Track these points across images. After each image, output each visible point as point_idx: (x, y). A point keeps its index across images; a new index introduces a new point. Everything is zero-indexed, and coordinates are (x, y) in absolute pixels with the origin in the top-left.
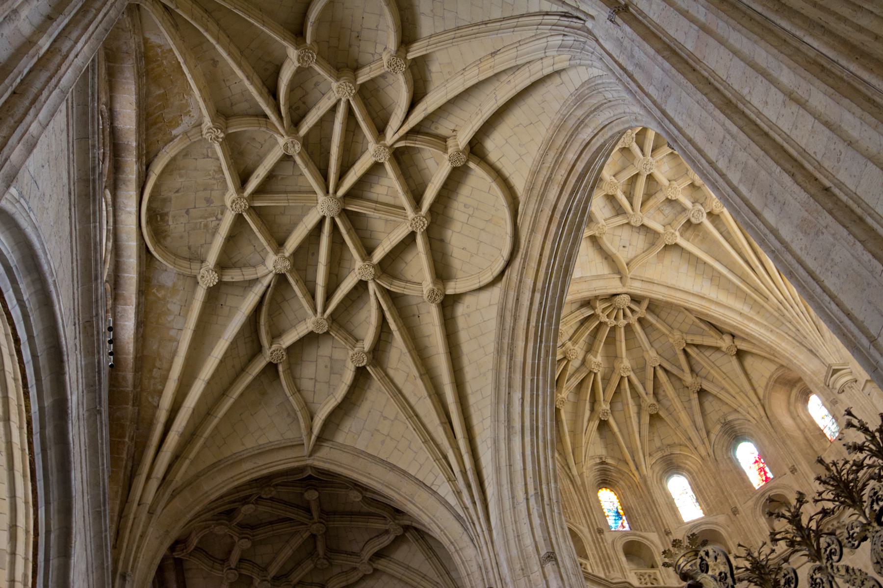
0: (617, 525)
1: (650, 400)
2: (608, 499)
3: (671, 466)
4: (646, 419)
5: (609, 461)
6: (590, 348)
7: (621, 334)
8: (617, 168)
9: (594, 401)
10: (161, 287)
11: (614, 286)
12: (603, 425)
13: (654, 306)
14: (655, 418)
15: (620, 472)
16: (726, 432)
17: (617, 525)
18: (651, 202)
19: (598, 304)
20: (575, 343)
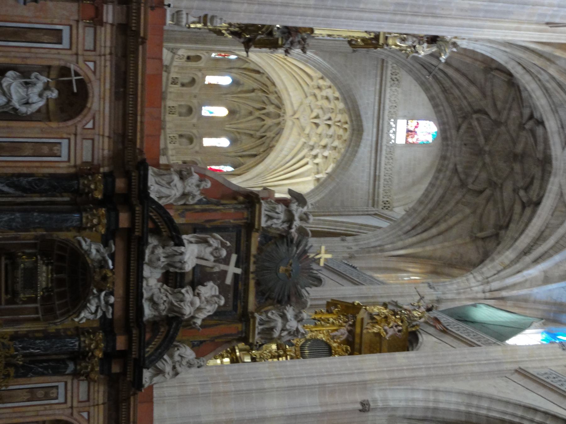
0: (206, 111)
12: (251, 113)
17: (206, 111)
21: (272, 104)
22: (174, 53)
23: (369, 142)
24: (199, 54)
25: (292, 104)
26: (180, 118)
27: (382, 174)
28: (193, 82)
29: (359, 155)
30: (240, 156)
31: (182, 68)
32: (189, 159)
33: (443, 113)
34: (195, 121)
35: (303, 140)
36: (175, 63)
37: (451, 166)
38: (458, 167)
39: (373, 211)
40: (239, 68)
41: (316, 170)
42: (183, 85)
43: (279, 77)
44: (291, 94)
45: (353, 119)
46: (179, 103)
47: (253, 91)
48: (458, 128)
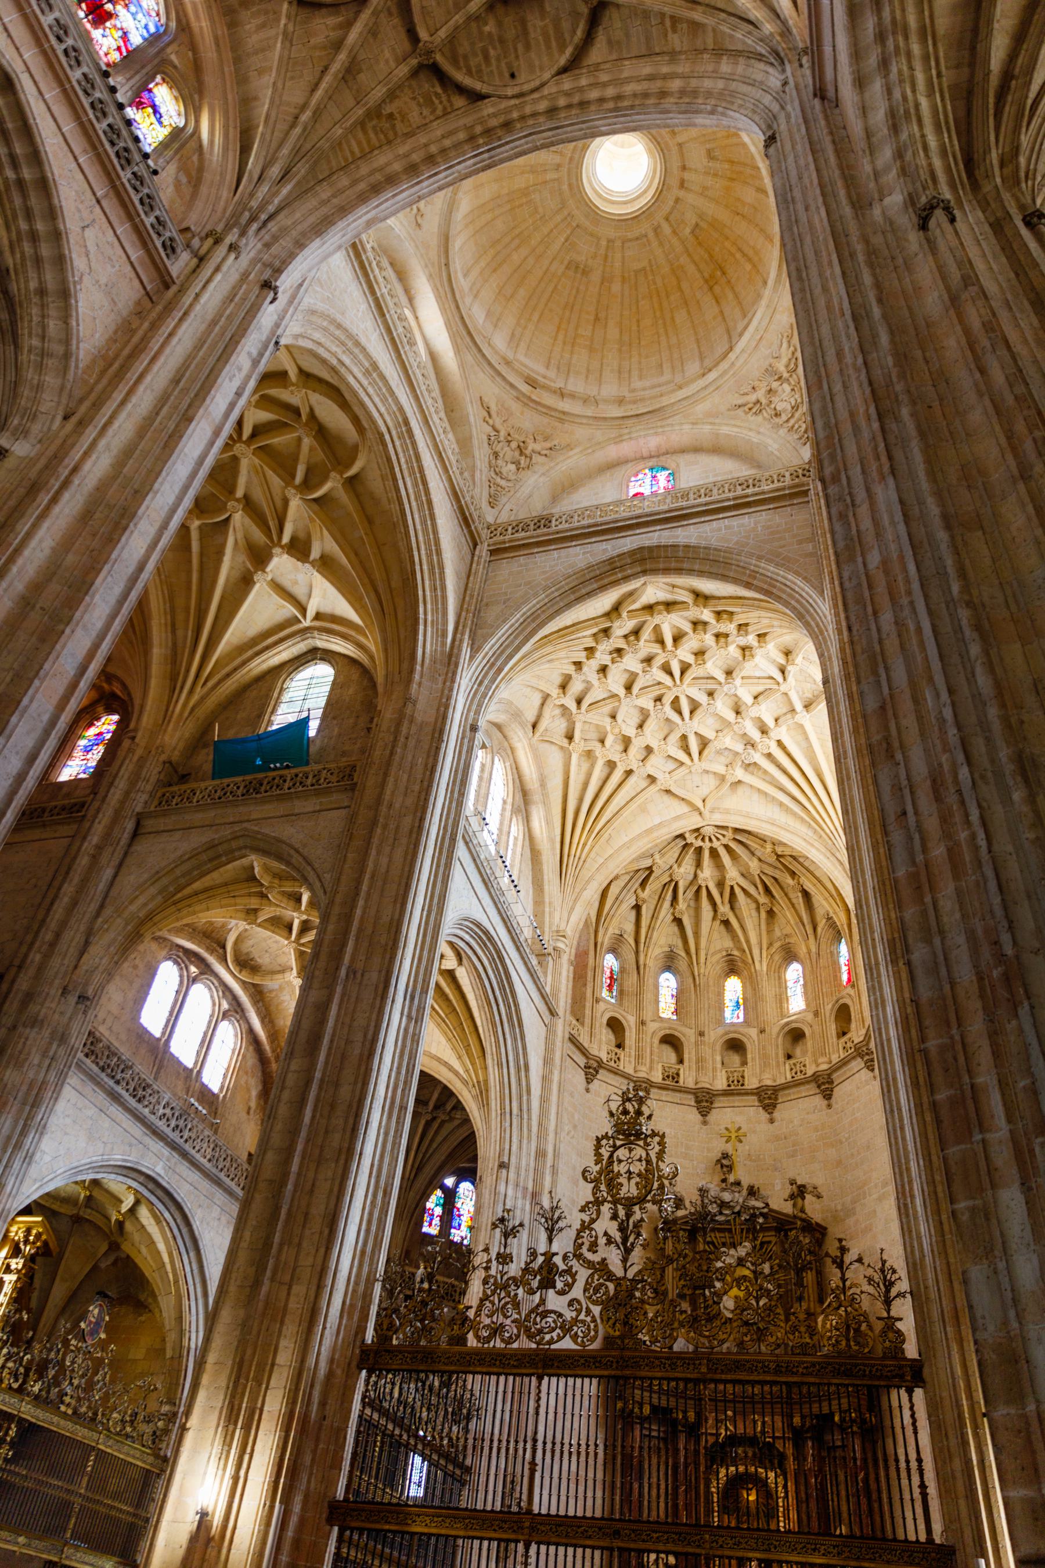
0: (733, 1016)
1: (763, 899)
2: (733, 987)
3: (789, 955)
4: (763, 915)
5: (736, 953)
6: (698, 864)
7: (722, 852)
8: (666, 732)
9: (714, 905)
10: (271, 991)
11: (695, 822)
12: (726, 923)
13: (737, 830)
14: (771, 913)
15: (744, 962)
16: (830, 926)
18: (706, 752)
19: (687, 835)
20: (679, 866)
21: (696, 876)
22: (600, 1064)
23: (666, 533)
24: (605, 1021)
25: (677, 818)
26: (750, 1064)
27: (731, 495)
28: (671, 1041)
29: (693, 541)
30: (815, 929)
31: (639, 1057)
32: (834, 1027)
33: (447, 143)
34: (753, 1032)
35: (739, 773)
36: (630, 1070)
37: (567, 83)
38: (563, 61)
39: (816, 488)
40: (637, 952)
41: (789, 716)
42: (681, 1061)
43: (627, 846)
44: (657, 821)
45: (620, 576)
46: (719, 1065)
47: (678, 921)
48: (476, 97)
